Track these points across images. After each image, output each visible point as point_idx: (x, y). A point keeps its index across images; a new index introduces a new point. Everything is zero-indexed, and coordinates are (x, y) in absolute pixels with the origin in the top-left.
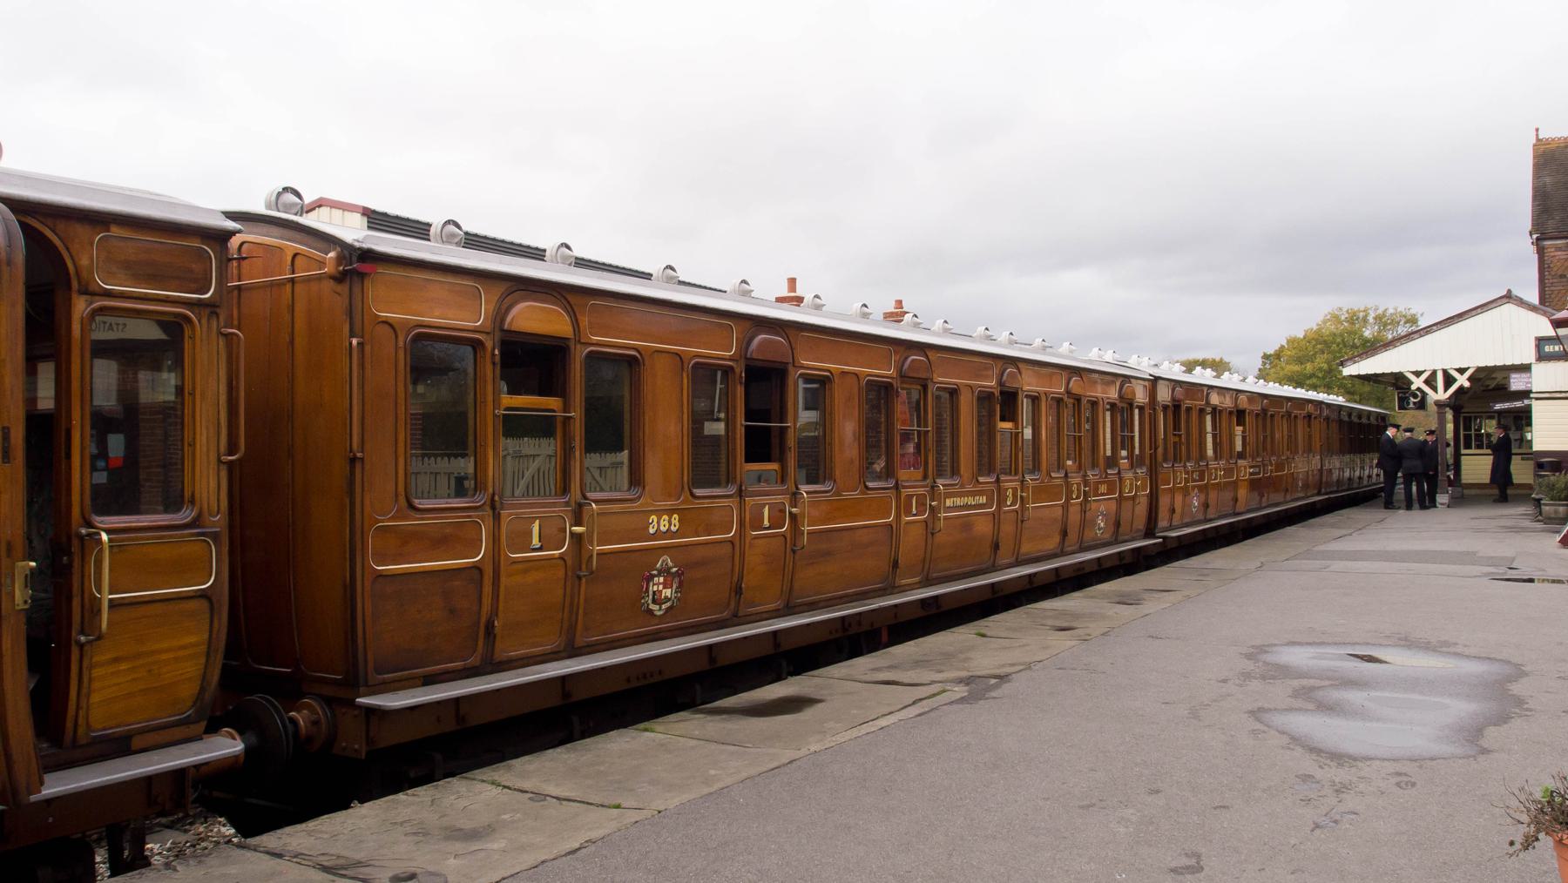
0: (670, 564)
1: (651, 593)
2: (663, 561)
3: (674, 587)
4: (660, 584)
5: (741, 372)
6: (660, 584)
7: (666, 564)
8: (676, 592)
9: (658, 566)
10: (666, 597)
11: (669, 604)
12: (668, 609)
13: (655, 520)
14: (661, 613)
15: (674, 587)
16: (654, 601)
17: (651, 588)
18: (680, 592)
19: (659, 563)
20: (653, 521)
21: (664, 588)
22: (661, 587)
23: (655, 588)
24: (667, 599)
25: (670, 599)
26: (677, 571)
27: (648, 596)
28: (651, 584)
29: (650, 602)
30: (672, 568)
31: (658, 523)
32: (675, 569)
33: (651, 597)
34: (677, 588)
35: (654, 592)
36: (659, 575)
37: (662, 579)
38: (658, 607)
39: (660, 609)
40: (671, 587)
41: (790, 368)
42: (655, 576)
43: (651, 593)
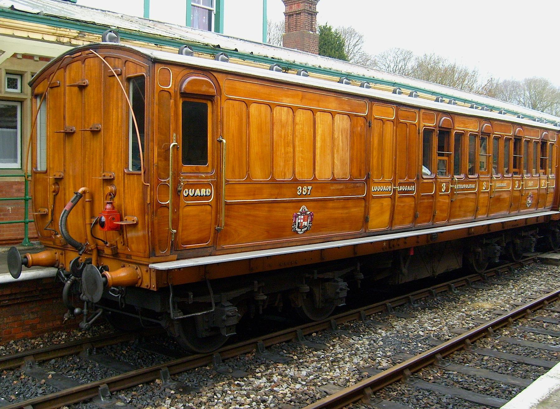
1: (297, 223)
3: (309, 221)
4: (302, 219)
6: (302, 219)
7: (304, 210)
8: (309, 223)
10: (304, 226)
11: (305, 229)
12: (305, 232)
13: (301, 188)
14: (302, 233)
15: (309, 221)
16: (298, 227)
17: (297, 221)
18: (311, 223)
20: (299, 189)
22: (302, 221)
23: (299, 221)
24: (305, 227)
26: (310, 213)
27: (296, 225)
28: (297, 219)
29: (296, 227)
31: (302, 189)
32: (308, 213)
33: (297, 225)
35: (299, 223)
36: (301, 215)
39: (301, 231)
42: (299, 215)
43: (297, 223)
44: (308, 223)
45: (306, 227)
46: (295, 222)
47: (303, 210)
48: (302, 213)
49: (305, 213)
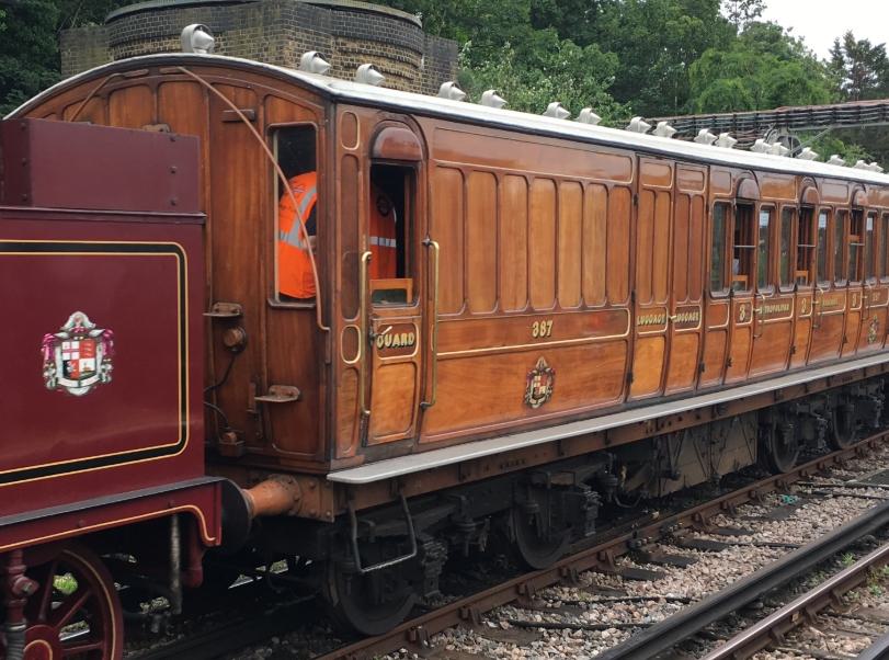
0: (89, 324)
2: (77, 320)
3: (100, 356)
4: (75, 351)
6: (75, 351)
7: (82, 325)
8: (103, 363)
10: (87, 370)
11: (94, 379)
16: (66, 374)
21: (83, 356)
22: (76, 356)
23: (66, 357)
25: (94, 373)
26: (101, 334)
27: (55, 367)
28: (58, 350)
29: (60, 374)
30: (91, 329)
32: (96, 332)
33: (60, 369)
34: (104, 357)
35: (65, 364)
37: (76, 345)
38: (75, 383)
39: (79, 387)
40: (94, 356)
44: (99, 362)
45: (94, 373)
48: (71, 337)
49: (86, 333)
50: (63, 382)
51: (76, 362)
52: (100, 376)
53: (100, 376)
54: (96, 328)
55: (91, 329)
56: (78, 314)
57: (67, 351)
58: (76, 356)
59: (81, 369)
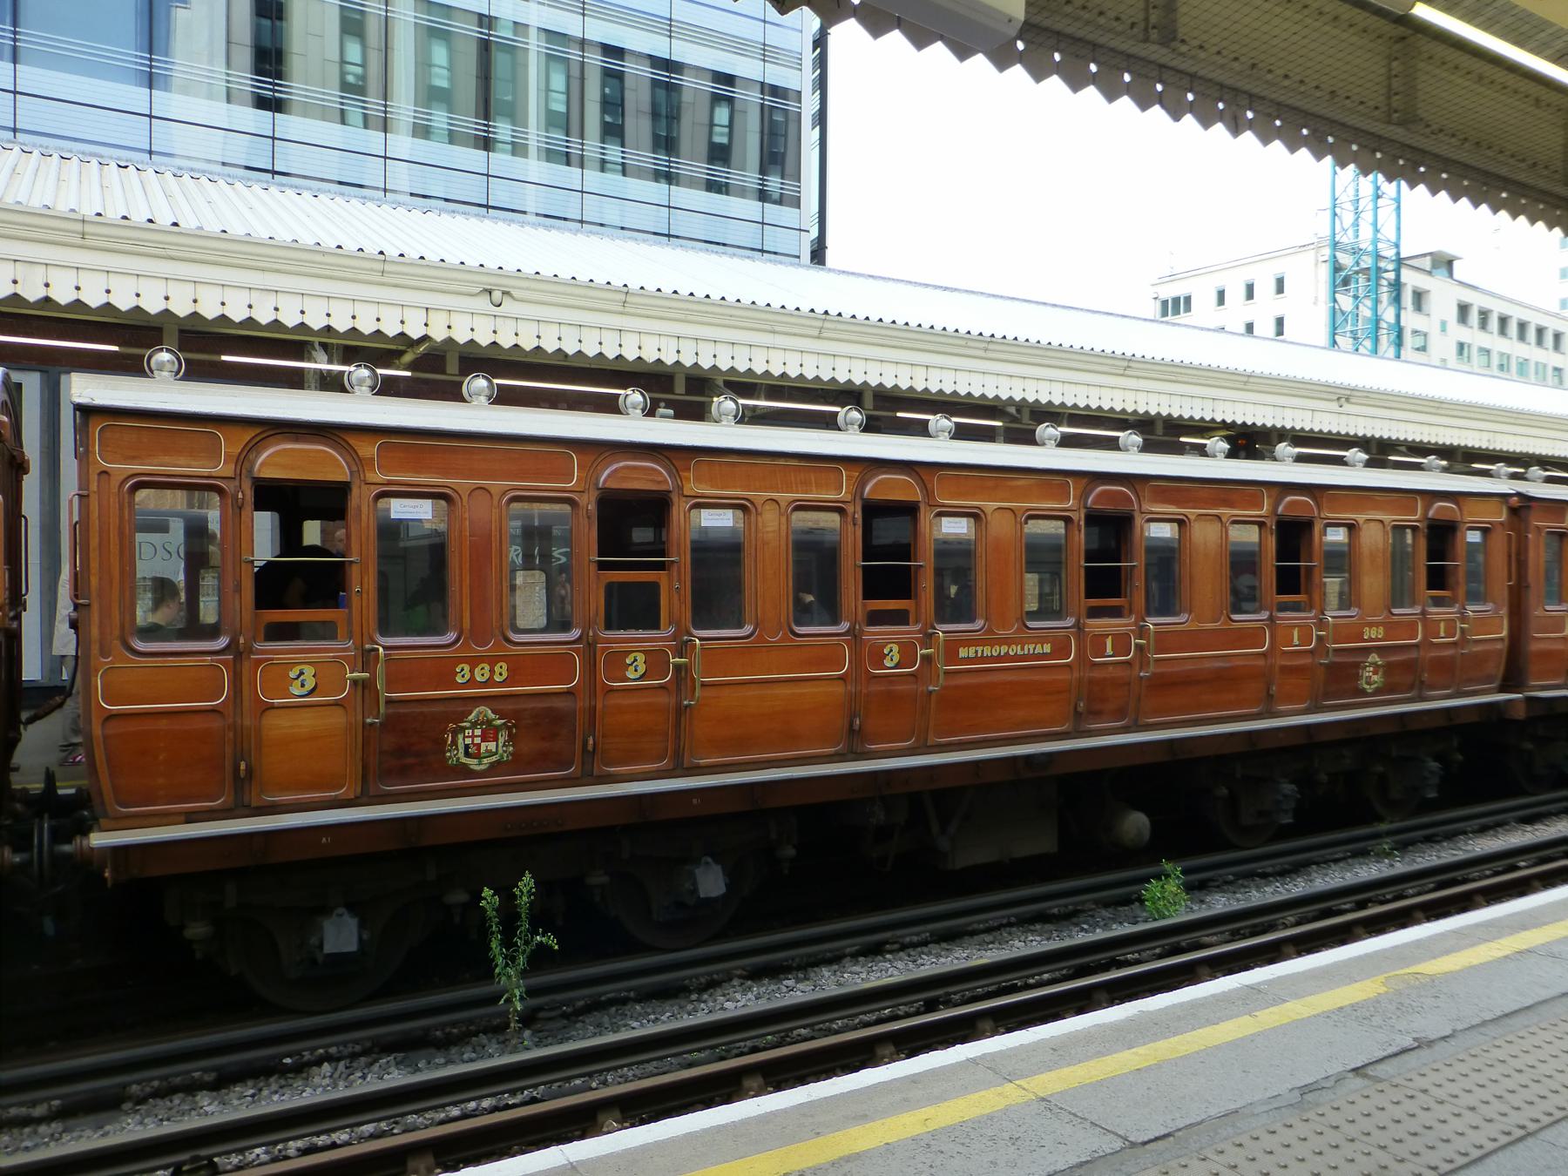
0: (491, 715)
3: (501, 740)
5: (1079, 521)
7: (485, 716)
8: (504, 745)
9: (470, 718)
11: (494, 759)
13: (467, 668)
14: (482, 767)
15: (501, 740)
16: (467, 754)
17: (460, 740)
19: (473, 714)
20: (462, 670)
23: (468, 741)
26: (504, 724)
27: (457, 749)
28: (460, 737)
30: (494, 720)
31: (472, 671)
33: (462, 750)
34: (505, 741)
35: (467, 747)
38: (476, 761)
40: (496, 740)
41: (675, 498)
42: (468, 728)
44: (500, 745)
45: (496, 753)
46: (454, 742)
47: (482, 716)
48: (474, 725)
49: (489, 722)
50: (464, 760)
51: (479, 746)
52: (502, 756)
53: (502, 756)
54: (499, 719)
55: (494, 720)
56: (482, 708)
57: (468, 737)
58: (477, 740)
59: (483, 749)
